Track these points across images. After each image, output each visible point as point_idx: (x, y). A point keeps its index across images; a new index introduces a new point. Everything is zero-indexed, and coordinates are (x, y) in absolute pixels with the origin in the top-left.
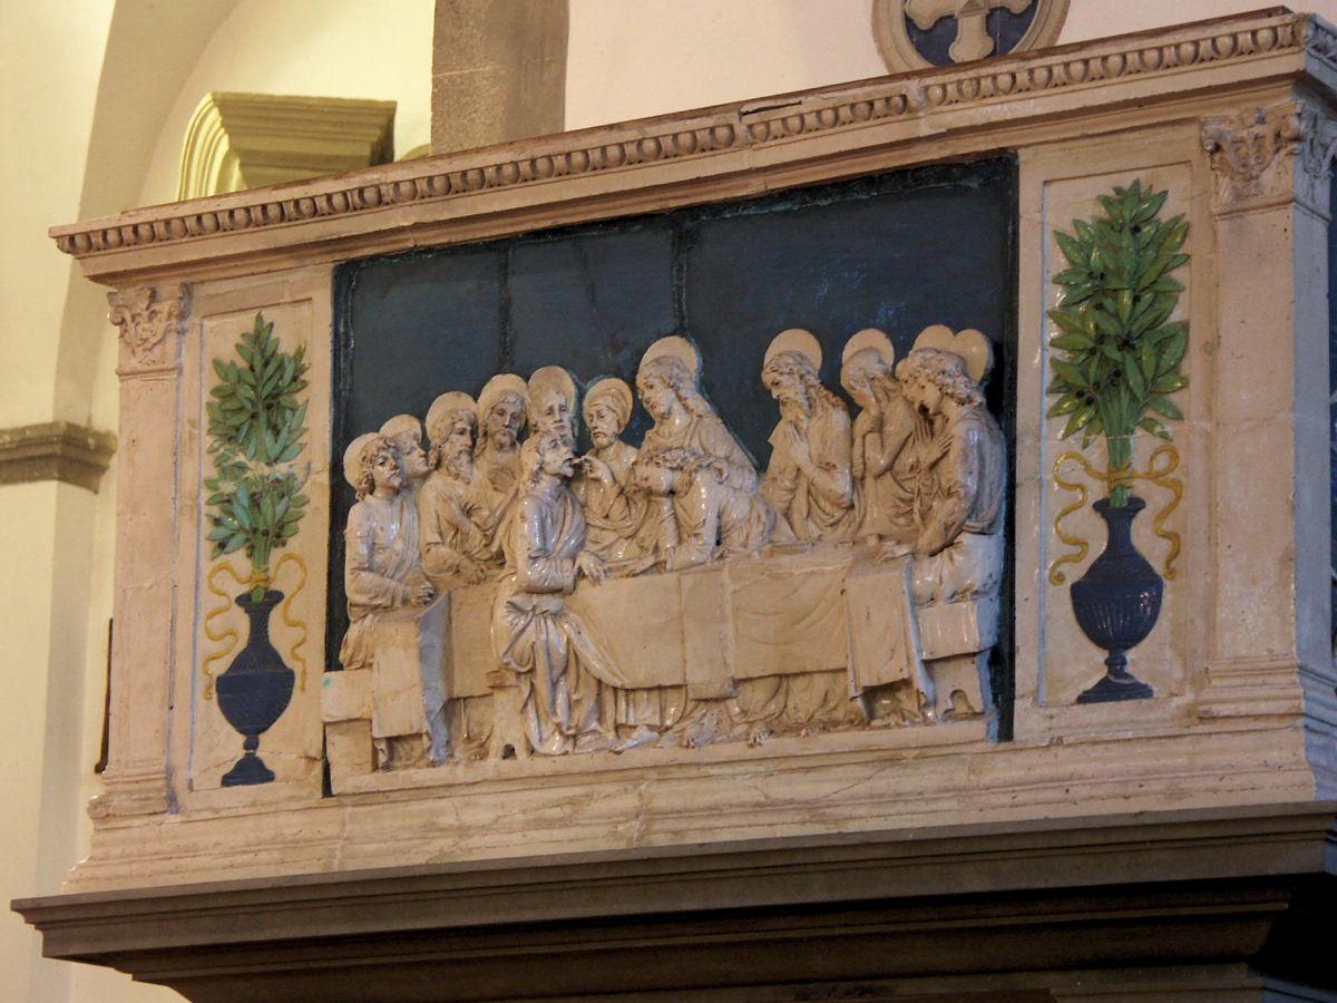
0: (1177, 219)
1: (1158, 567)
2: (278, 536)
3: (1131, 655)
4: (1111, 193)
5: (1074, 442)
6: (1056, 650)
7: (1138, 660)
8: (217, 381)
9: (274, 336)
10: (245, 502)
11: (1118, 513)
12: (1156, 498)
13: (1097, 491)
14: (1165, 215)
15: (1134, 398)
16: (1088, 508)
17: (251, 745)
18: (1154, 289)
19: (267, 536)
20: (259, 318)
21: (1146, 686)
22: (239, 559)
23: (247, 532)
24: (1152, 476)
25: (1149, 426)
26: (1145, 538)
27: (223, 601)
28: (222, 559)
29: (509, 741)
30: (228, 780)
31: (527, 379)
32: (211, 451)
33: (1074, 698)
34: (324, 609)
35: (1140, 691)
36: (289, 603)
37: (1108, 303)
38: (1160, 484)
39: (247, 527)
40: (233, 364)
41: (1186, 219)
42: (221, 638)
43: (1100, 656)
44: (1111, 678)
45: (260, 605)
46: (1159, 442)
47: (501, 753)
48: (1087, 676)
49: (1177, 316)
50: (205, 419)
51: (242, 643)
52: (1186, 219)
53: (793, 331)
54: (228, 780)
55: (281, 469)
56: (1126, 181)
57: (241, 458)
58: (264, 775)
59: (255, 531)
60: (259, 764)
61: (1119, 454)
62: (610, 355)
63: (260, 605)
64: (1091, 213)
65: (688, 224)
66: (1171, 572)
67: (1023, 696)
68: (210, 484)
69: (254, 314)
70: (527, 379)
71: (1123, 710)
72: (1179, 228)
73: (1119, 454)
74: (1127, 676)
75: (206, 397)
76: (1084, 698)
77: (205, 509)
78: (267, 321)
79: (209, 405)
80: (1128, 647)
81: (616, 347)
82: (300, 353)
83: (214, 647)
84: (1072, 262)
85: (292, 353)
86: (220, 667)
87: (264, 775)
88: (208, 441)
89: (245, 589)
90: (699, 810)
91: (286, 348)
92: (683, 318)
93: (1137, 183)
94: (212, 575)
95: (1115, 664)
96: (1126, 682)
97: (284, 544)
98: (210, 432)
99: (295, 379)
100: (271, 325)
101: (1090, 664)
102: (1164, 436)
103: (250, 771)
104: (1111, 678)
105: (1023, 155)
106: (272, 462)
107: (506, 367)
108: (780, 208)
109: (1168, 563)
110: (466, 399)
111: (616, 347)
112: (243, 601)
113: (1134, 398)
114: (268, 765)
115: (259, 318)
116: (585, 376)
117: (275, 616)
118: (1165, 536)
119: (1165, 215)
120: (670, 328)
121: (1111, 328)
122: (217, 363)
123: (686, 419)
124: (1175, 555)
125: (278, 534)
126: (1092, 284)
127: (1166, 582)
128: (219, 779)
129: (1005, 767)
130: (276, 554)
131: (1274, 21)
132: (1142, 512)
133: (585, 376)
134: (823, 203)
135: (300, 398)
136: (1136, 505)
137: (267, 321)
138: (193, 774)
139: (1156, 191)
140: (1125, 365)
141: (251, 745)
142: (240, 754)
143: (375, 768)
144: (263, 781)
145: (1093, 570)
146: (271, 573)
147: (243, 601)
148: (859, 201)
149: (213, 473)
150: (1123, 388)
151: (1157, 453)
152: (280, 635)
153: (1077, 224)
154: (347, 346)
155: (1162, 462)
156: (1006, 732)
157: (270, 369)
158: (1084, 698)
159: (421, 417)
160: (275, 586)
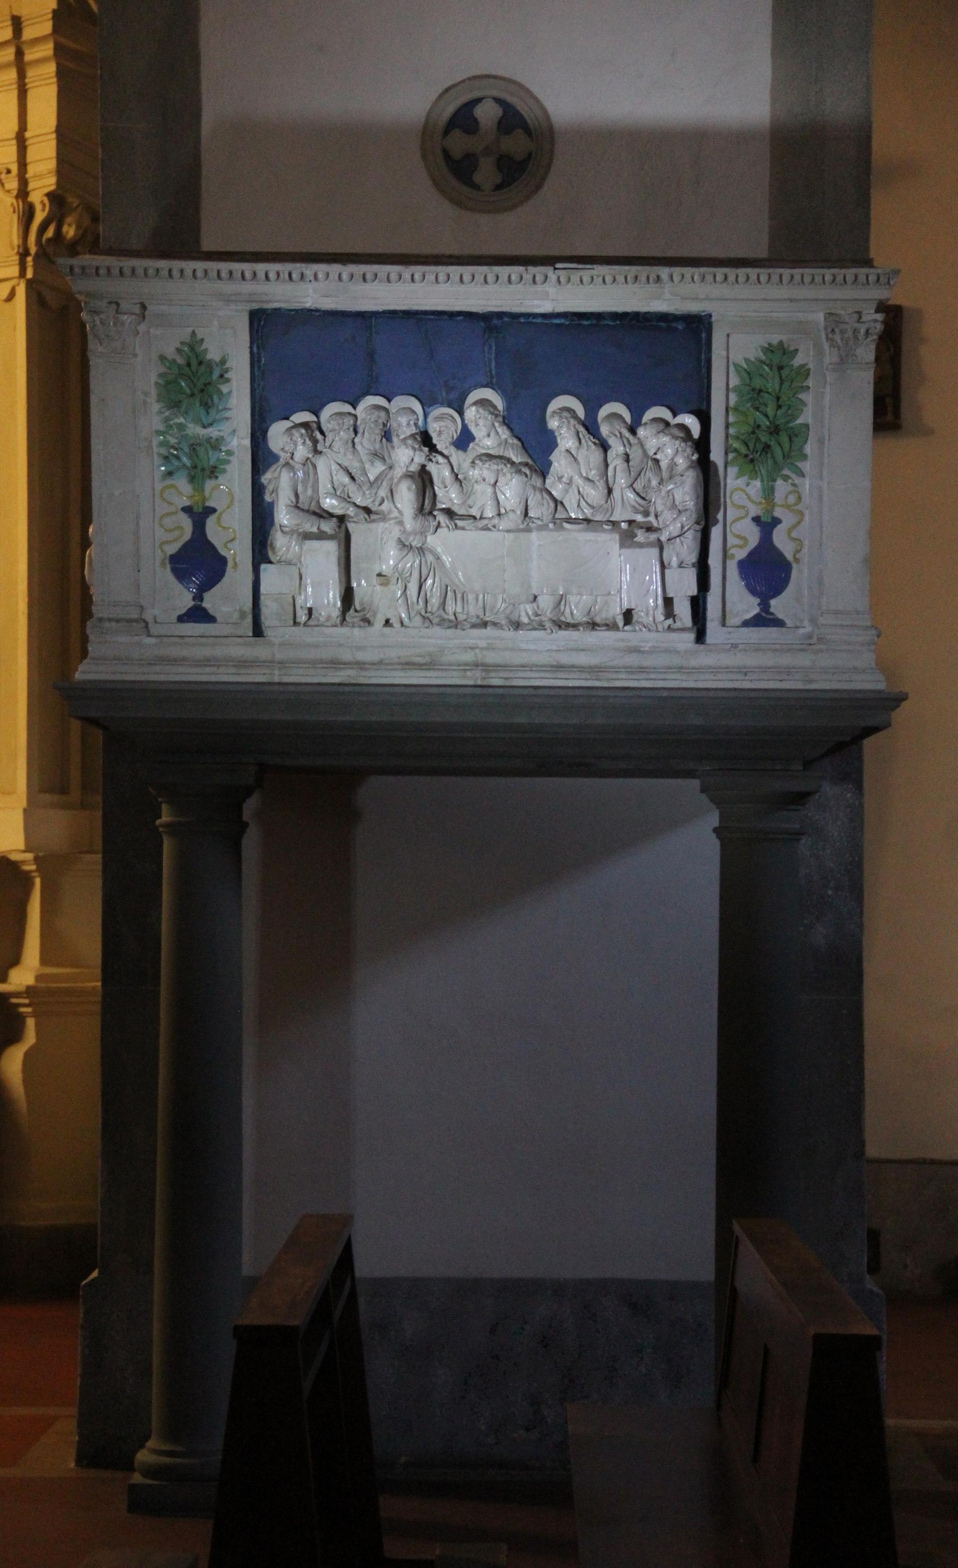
0: (803, 366)
1: (789, 556)
2: (212, 472)
3: (773, 602)
4: (766, 345)
6: (734, 597)
7: (777, 605)
8: (162, 369)
9: (204, 347)
10: (187, 450)
11: (767, 525)
12: (787, 519)
13: (754, 511)
14: (798, 361)
15: (775, 462)
16: (748, 520)
17: (199, 597)
18: (786, 403)
21: (782, 620)
22: (182, 483)
23: (188, 468)
24: (788, 507)
25: (786, 478)
26: (780, 539)
27: (173, 509)
28: (169, 482)
29: (389, 616)
30: (181, 619)
32: (160, 412)
33: (739, 623)
34: (251, 523)
35: (778, 623)
36: (221, 514)
37: (762, 408)
38: (792, 511)
39: (188, 464)
40: (174, 361)
41: (807, 367)
42: (171, 531)
43: (755, 601)
44: (764, 615)
46: (792, 488)
47: (383, 622)
48: (748, 612)
52: (807, 367)
53: (566, 396)
54: (181, 619)
55: (213, 432)
56: (775, 339)
57: (182, 420)
58: (207, 617)
59: (195, 467)
60: (204, 610)
61: (769, 493)
62: (444, 393)
63: (200, 515)
64: (754, 353)
65: (495, 321)
66: (797, 560)
67: (712, 620)
68: (159, 433)
71: (770, 633)
72: (804, 372)
73: (769, 493)
74: (772, 614)
75: (153, 378)
76: (746, 624)
78: (199, 336)
79: (156, 383)
80: (774, 597)
81: (450, 389)
82: (223, 361)
84: (742, 379)
85: (217, 359)
86: (173, 549)
87: (207, 617)
88: (156, 407)
89: (187, 503)
90: (517, 666)
91: (213, 355)
92: (492, 377)
93: (781, 343)
94: (162, 491)
95: (765, 606)
96: (771, 617)
97: (217, 477)
98: (158, 401)
99: (222, 376)
100: (202, 340)
101: (748, 606)
102: (794, 485)
103: (198, 614)
104: (764, 615)
107: (373, 391)
109: (794, 556)
110: (347, 408)
111: (450, 389)
112: (187, 510)
113: (775, 462)
114: (211, 612)
116: (428, 402)
117: (211, 522)
118: (794, 540)
119: (798, 361)
122: (162, 358)
123: (489, 435)
124: (798, 551)
125: (213, 472)
126: (754, 394)
127: (794, 566)
129: (704, 658)
130: (209, 484)
132: (779, 526)
133: (428, 402)
134: (585, 323)
135: (225, 389)
136: (776, 522)
137: (199, 336)
138: (156, 612)
139: (792, 348)
140: (772, 442)
141: (199, 597)
143: (295, 623)
144: (209, 622)
145: (751, 554)
146: (207, 494)
147: (187, 510)
148: (608, 325)
149: (161, 427)
150: (769, 455)
151: (791, 492)
153: (746, 360)
154: (259, 361)
155: (792, 499)
156: (700, 637)
157: (203, 368)
158: (746, 624)
159: (316, 413)
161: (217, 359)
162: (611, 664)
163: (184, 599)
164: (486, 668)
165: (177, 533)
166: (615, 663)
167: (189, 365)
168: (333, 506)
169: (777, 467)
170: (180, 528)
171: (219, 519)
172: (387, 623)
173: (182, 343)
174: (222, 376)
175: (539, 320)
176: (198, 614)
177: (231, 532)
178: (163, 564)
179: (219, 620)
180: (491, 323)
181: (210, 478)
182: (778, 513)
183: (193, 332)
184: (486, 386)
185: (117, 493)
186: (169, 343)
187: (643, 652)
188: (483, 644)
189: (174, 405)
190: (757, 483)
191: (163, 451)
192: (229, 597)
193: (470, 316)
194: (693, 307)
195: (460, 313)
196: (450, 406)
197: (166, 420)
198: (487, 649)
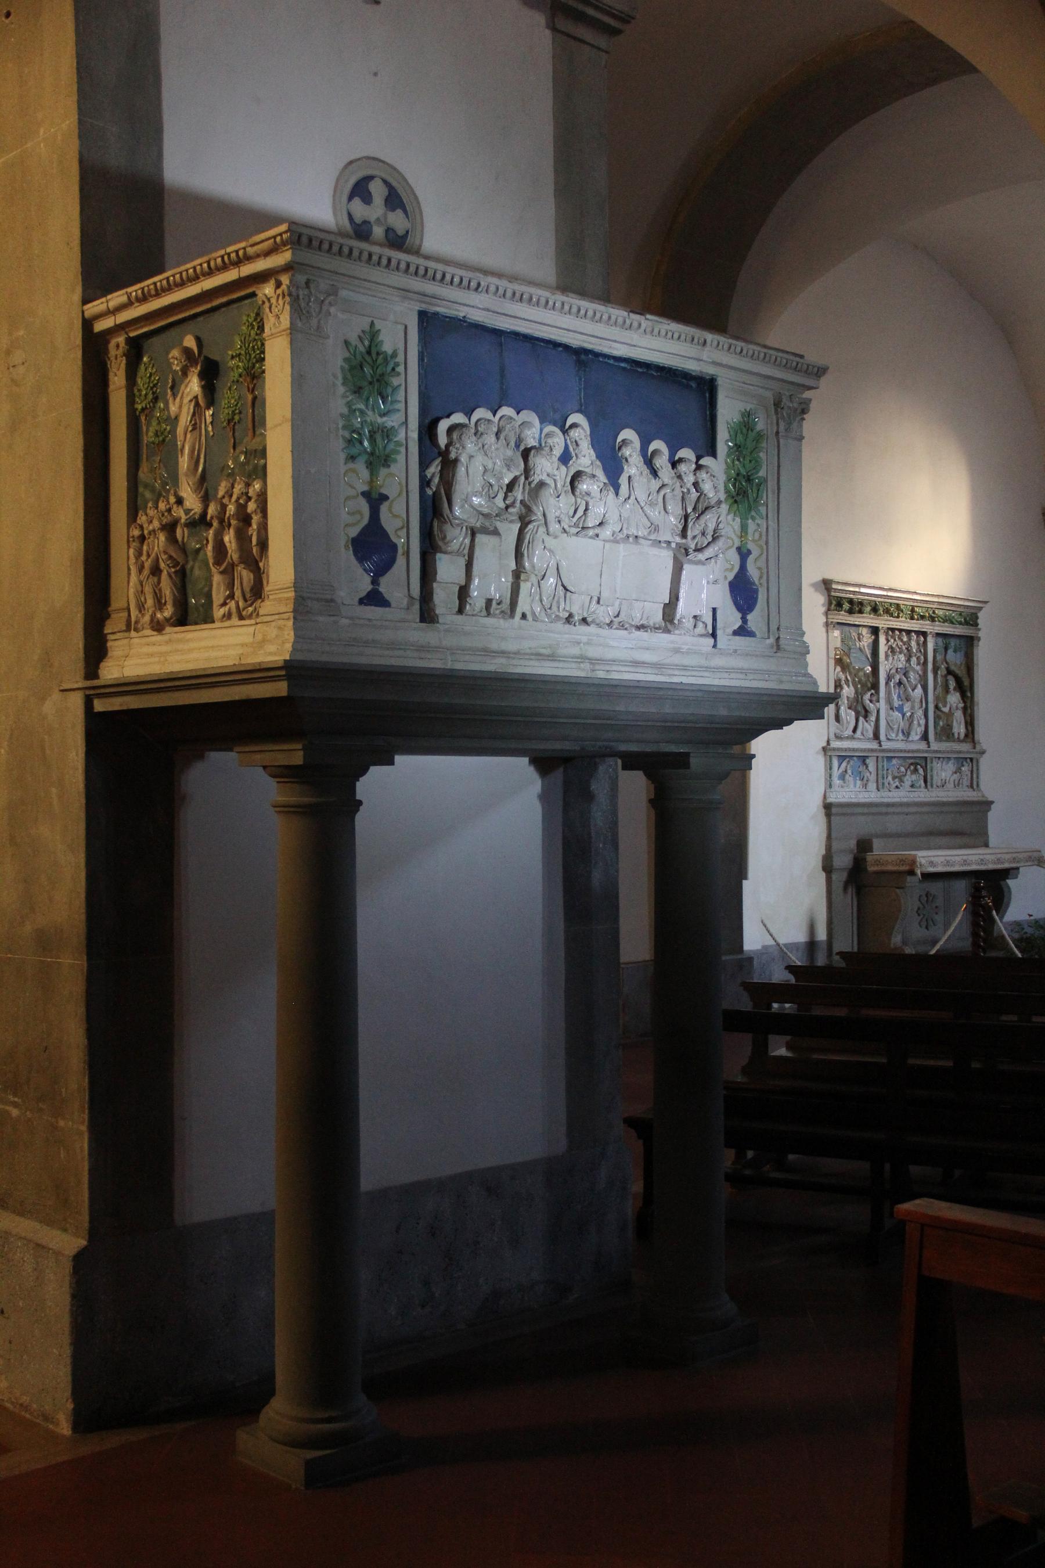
2: (385, 460)
5: (730, 517)
16: (734, 549)
19: (378, 461)
20: (372, 323)
22: (361, 466)
27: (351, 492)
28: (351, 465)
30: (361, 602)
31: (518, 413)
32: (344, 396)
45: (375, 500)
49: (762, 473)
50: (340, 376)
51: (365, 521)
54: (361, 602)
57: (362, 406)
63: (375, 500)
65: (583, 357)
69: (370, 320)
70: (518, 413)
75: (340, 362)
77: (341, 432)
79: (342, 368)
82: (395, 355)
83: (350, 519)
85: (390, 352)
86: (354, 532)
87: (384, 603)
88: (341, 390)
89: (365, 488)
91: (387, 348)
95: (744, 620)
97: (389, 466)
99: (393, 369)
103: (374, 598)
105: (720, 382)
106: (383, 415)
108: (623, 365)
115: (372, 323)
117: (384, 508)
120: (576, 408)
121: (743, 472)
122: (347, 343)
125: (386, 461)
128: (357, 600)
130: (383, 472)
131: (798, 359)
134: (640, 370)
136: (749, 552)
141: (375, 582)
142: (370, 587)
149: (345, 411)
152: (389, 521)
160: (384, 491)
161: (390, 352)
162: (665, 662)
163: (365, 585)
164: (593, 661)
165: (358, 517)
166: (667, 661)
167: (369, 353)
168: (480, 505)
169: (750, 509)
170: (360, 513)
171: (390, 507)
172: (524, 616)
173: (363, 331)
174: (393, 369)
175: (611, 362)
176: (374, 598)
177: (402, 520)
178: (346, 547)
179: (393, 604)
180: (583, 358)
181: (384, 466)
183: (372, 322)
184: (577, 412)
185: (313, 471)
186: (354, 328)
187: (683, 653)
188: (584, 639)
189: (358, 391)
190: (738, 520)
191: (347, 434)
192: (400, 582)
193: (567, 348)
194: (710, 370)
195: (560, 345)
196: (555, 425)
197: (349, 405)
198: (588, 643)
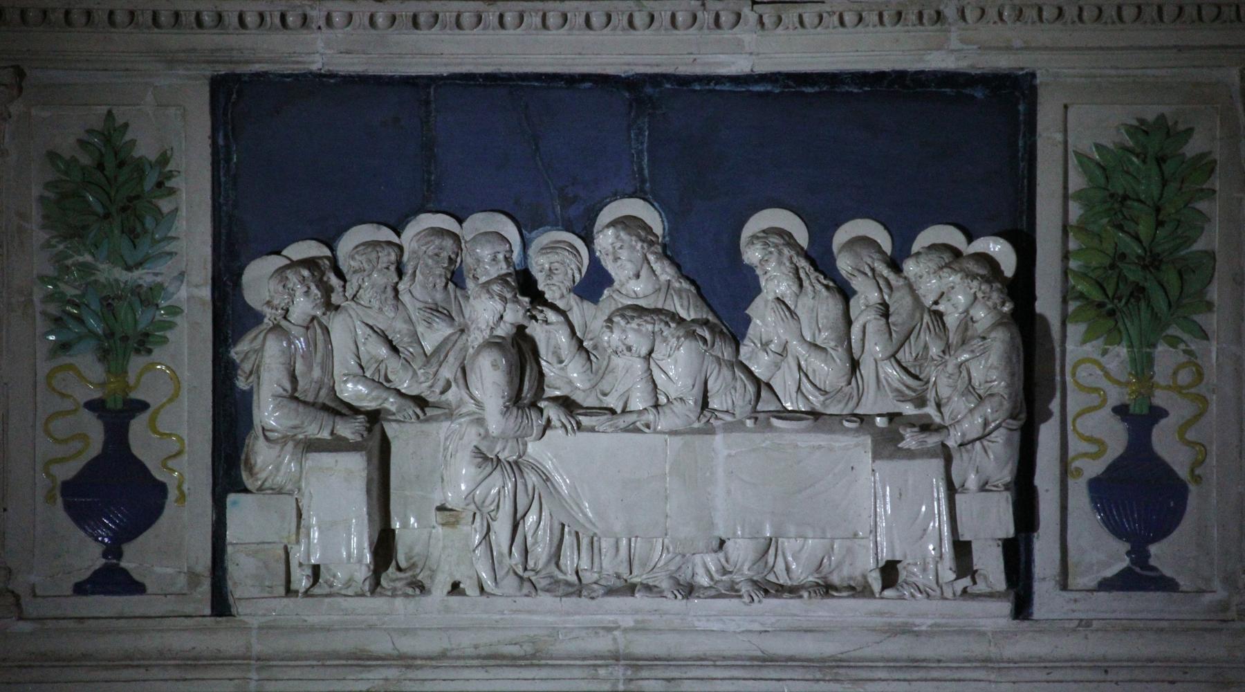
0: (1202, 156)
1: (1183, 473)
3: (1153, 549)
11: (1140, 420)
15: (1155, 316)
22: (87, 363)
25: (1174, 342)
28: (65, 360)
32: (48, 245)
42: (65, 441)
61: (1143, 367)
74: (1154, 569)
82: (164, 160)
85: (153, 156)
88: (43, 236)
91: (146, 149)
97: (149, 352)
98: (43, 227)
99: (160, 185)
100: (126, 125)
109: (1192, 471)
113: (1155, 316)
116: (528, 224)
127: (1192, 488)
133: (528, 224)
136: (1158, 414)
137: (120, 121)
139: (1181, 127)
151: (1181, 366)
155: (1184, 377)
182: (1160, 399)
